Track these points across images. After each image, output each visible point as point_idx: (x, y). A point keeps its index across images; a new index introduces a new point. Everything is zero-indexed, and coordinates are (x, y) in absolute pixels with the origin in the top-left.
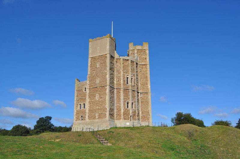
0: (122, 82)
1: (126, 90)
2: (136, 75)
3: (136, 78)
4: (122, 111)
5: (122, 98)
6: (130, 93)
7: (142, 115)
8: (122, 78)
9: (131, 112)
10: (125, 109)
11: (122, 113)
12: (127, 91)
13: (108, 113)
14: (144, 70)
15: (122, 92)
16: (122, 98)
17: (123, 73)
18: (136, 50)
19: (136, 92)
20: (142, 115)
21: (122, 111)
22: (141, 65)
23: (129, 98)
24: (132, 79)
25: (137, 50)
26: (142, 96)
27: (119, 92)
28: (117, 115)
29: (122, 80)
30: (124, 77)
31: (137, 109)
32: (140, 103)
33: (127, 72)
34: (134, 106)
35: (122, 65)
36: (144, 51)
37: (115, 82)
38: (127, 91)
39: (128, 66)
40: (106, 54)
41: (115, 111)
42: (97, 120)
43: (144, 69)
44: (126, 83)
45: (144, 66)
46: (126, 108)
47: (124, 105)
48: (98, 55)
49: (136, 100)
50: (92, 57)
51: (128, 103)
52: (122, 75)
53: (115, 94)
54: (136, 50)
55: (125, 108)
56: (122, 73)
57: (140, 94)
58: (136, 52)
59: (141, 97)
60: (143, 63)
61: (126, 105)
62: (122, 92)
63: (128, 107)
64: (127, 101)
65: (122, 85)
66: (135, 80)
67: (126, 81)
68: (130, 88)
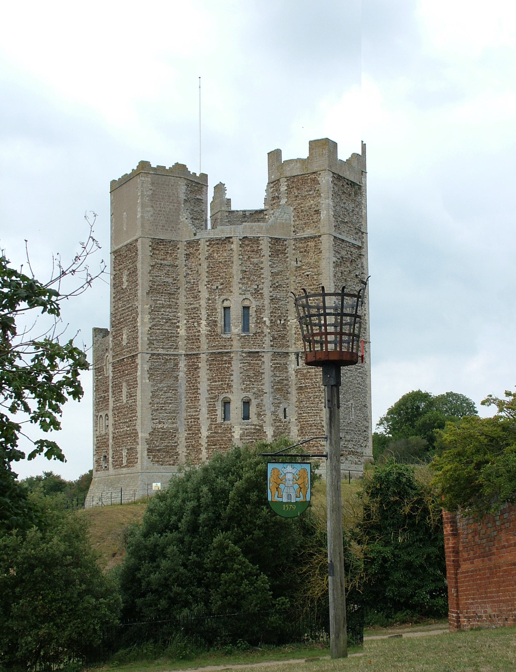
0: (204, 329)
1: (220, 359)
2: (266, 291)
3: (267, 302)
4: (204, 433)
5: (204, 386)
6: (236, 366)
7: (299, 438)
8: (204, 314)
9: (237, 433)
10: (213, 426)
11: (204, 442)
12: (225, 358)
13: (141, 449)
14: (311, 258)
15: (203, 365)
16: (204, 386)
17: (210, 293)
18: (283, 181)
19: (267, 358)
20: (299, 438)
21: (204, 433)
22: (301, 239)
23: (230, 386)
24: (246, 309)
25: (288, 179)
26: (300, 367)
27: (193, 368)
28: (187, 447)
29: (204, 322)
30: (211, 310)
31: (268, 418)
32: (293, 391)
33: (227, 286)
34: (253, 410)
35: (205, 265)
36: (314, 180)
37: (182, 332)
38: (225, 358)
39: (228, 263)
40: (134, 238)
41: (182, 435)
42: (124, 470)
43: (311, 254)
44: (219, 330)
45: (312, 244)
46: (219, 420)
47: (212, 410)
48: (125, 243)
49: (267, 388)
50: (116, 248)
51: (226, 403)
52: (203, 303)
53: (182, 374)
54: (283, 181)
55: (213, 420)
56: (204, 294)
57: (293, 357)
58: (283, 188)
59: (297, 371)
60: (308, 232)
61: (220, 412)
62: (203, 365)
63: (226, 417)
64: (221, 397)
65: (203, 340)
66: (259, 310)
67: (221, 323)
68: (236, 345)
